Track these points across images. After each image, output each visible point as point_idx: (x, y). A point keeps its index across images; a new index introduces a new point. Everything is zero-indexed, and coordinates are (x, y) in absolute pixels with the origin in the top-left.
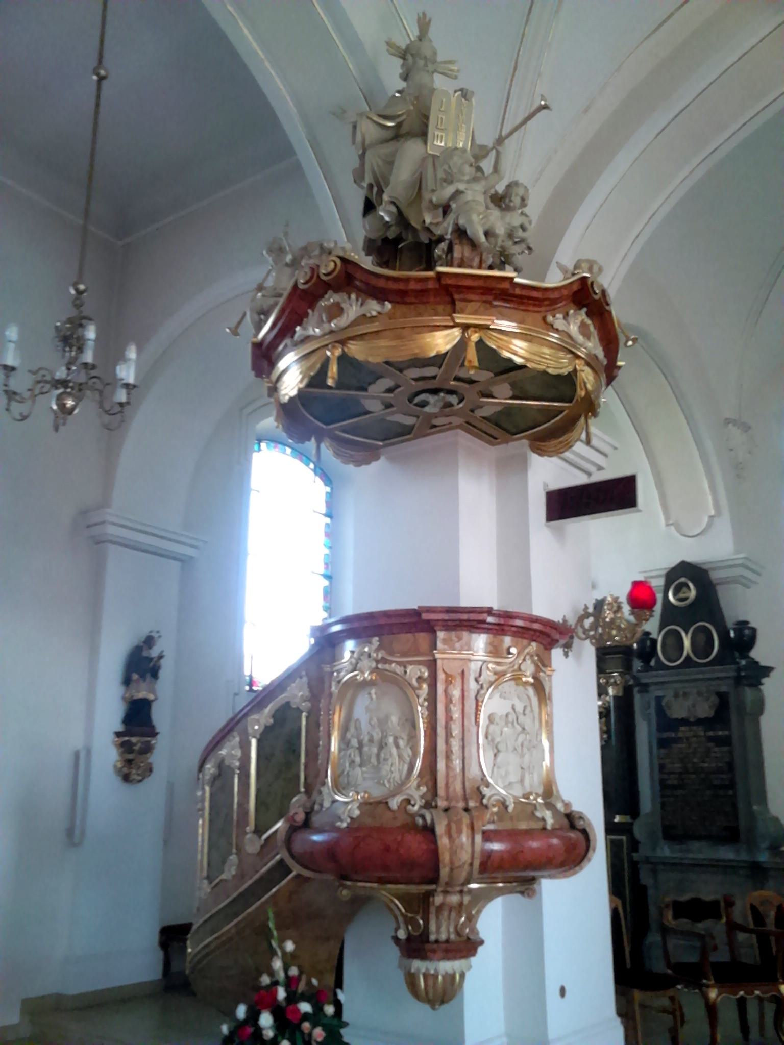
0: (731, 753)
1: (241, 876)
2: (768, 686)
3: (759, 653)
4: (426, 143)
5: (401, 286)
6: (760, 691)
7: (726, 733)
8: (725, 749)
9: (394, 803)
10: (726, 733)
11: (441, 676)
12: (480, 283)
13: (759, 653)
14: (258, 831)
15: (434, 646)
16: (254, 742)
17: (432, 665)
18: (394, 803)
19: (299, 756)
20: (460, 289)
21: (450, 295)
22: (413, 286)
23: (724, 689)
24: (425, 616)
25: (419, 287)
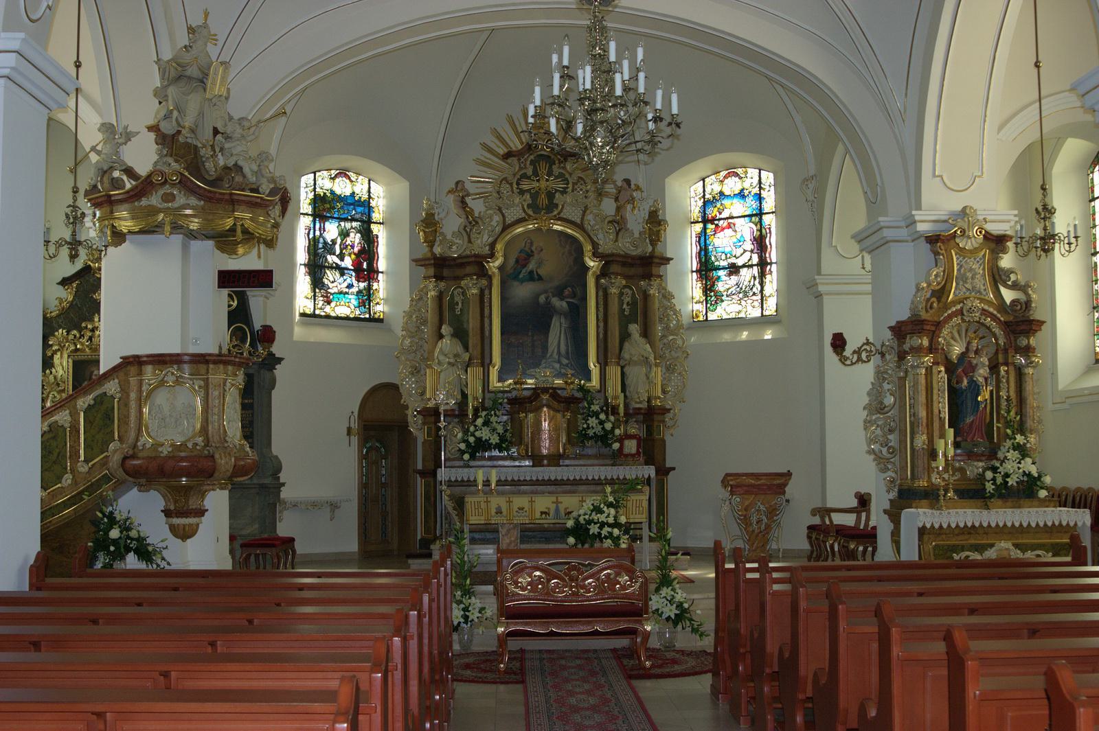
0: (253, 414)
1: (75, 482)
2: (279, 371)
3: (277, 349)
4: (205, 90)
5: (212, 195)
6: (273, 373)
7: (250, 401)
8: (250, 412)
9: (190, 445)
10: (250, 401)
11: (211, 386)
12: (248, 199)
13: (277, 349)
14: (86, 461)
15: (208, 372)
16: (82, 414)
17: (206, 381)
18: (190, 445)
19: (113, 421)
20: (238, 201)
21: (233, 202)
22: (217, 196)
23: (251, 371)
24: (207, 358)
25: (220, 197)
